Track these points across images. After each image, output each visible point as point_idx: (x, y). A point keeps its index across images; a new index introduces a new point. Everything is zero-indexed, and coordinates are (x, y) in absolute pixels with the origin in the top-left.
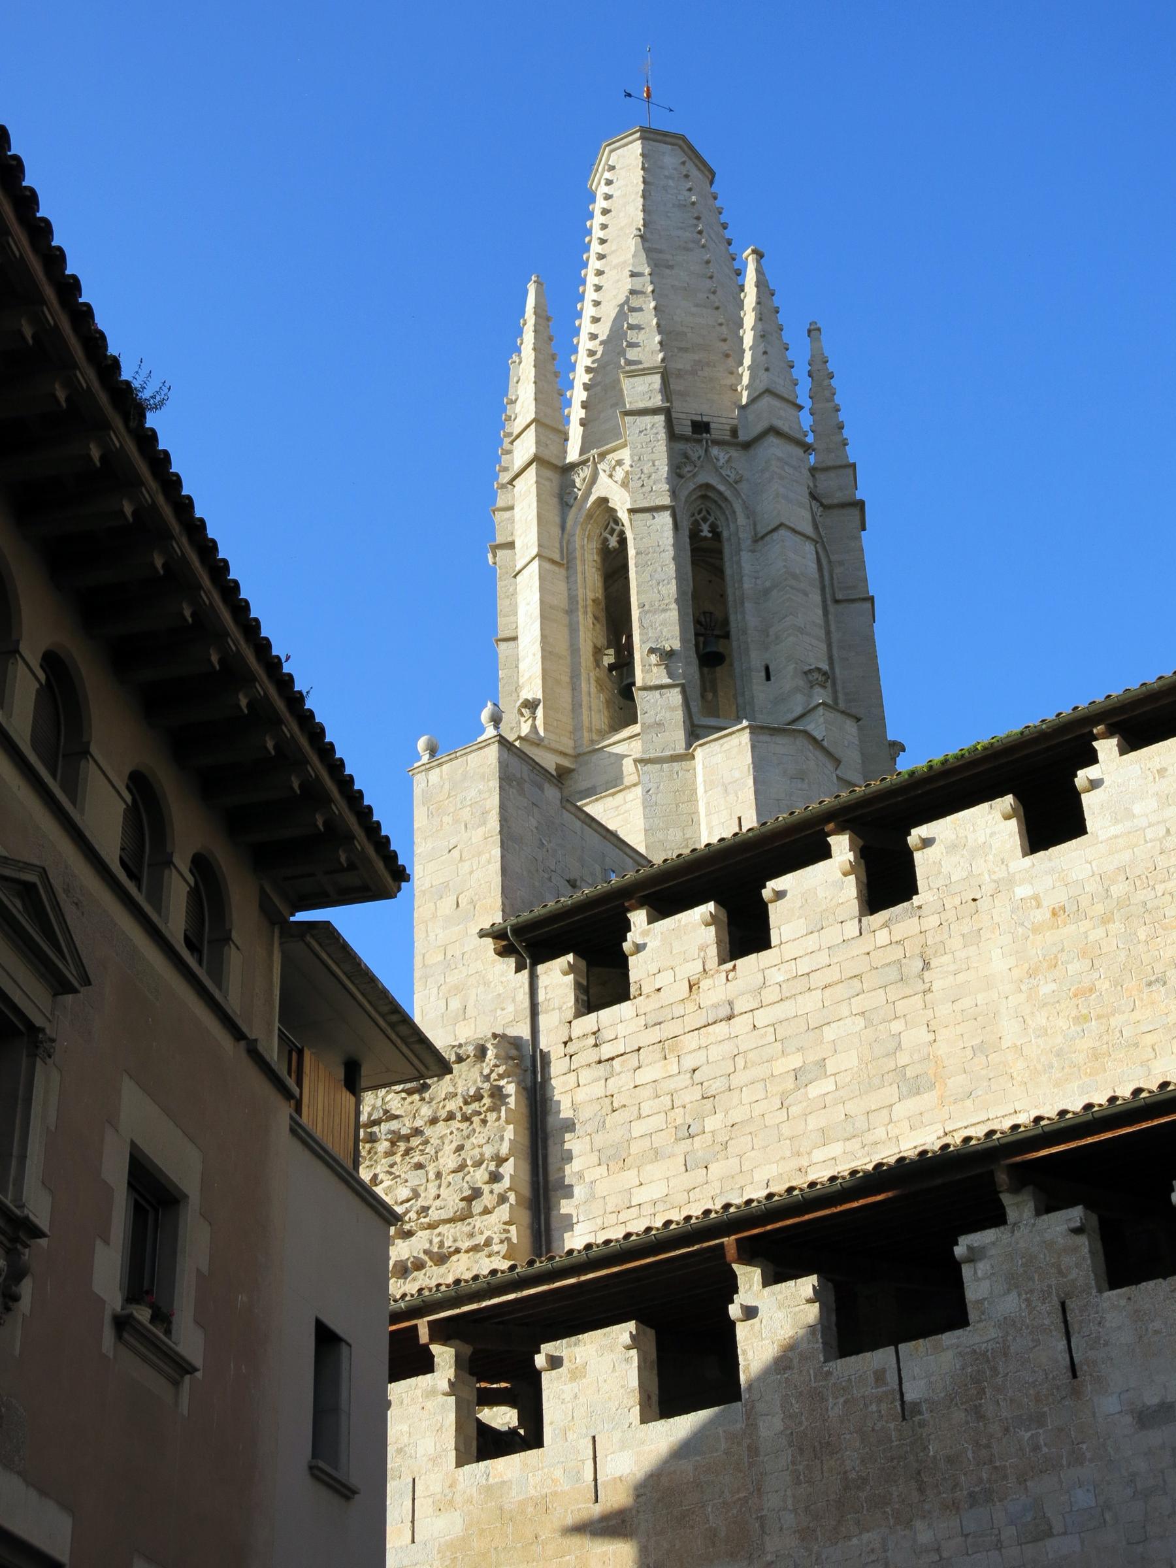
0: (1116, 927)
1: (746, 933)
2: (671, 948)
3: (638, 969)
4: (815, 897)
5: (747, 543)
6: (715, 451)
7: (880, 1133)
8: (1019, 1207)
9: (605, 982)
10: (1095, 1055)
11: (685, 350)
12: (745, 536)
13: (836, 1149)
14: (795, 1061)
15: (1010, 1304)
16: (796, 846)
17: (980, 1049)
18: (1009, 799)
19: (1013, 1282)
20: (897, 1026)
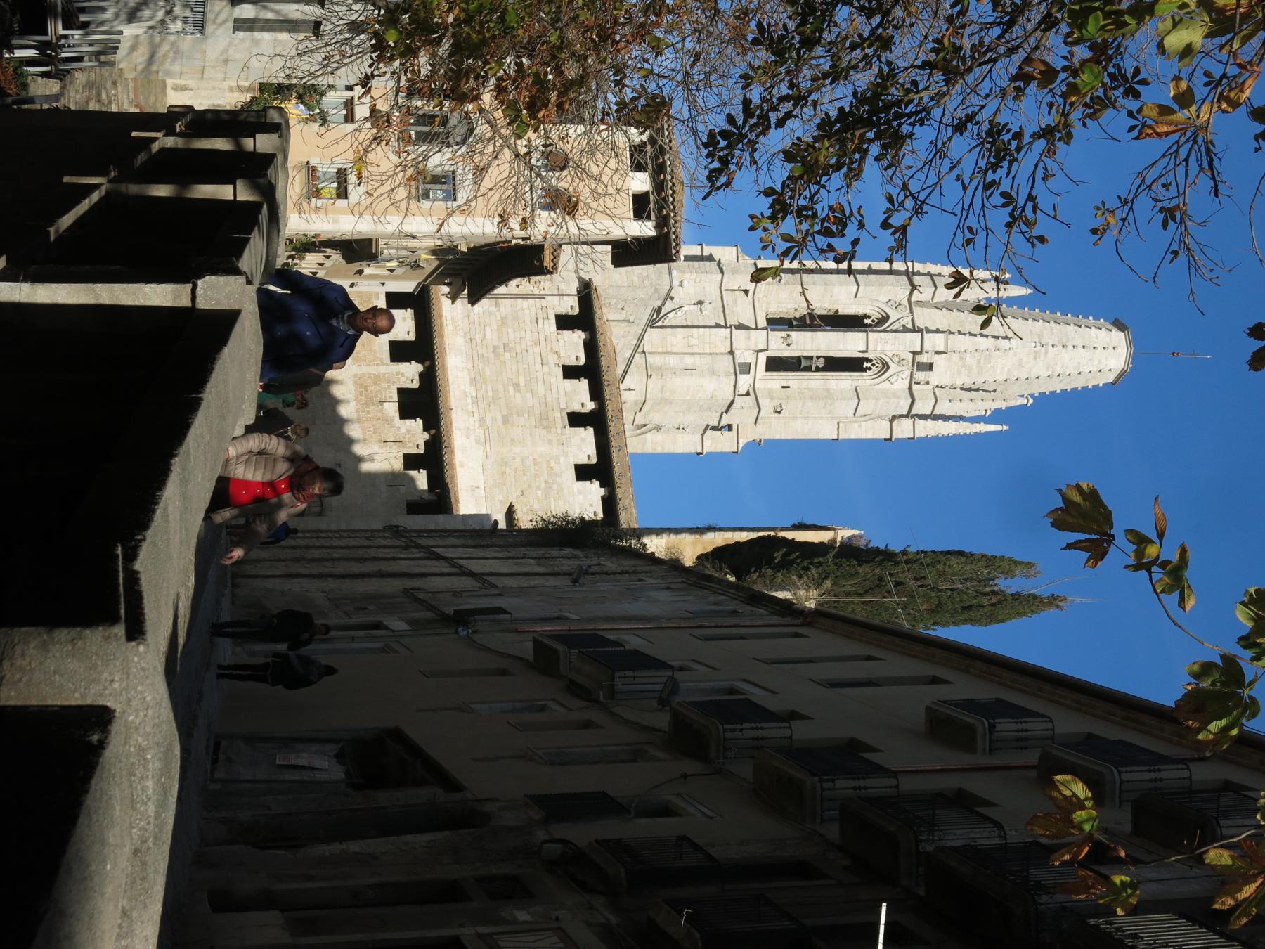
0: (543, 486)
1: (570, 372)
2: (572, 346)
3: (567, 334)
4: (579, 395)
5: (856, 383)
6: (908, 373)
7: (492, 407)
8: (426, 436)
9: (564, 322)
10: (503, 473)
11: (979, 362)
12: (860, 383)
13: (490, 394)
14: (522, 384)
15: (403, 430)
16: (597, 393)
17: (513, 440)
18: (594, 461)
19: (409, 431)
20: (526, 416)
